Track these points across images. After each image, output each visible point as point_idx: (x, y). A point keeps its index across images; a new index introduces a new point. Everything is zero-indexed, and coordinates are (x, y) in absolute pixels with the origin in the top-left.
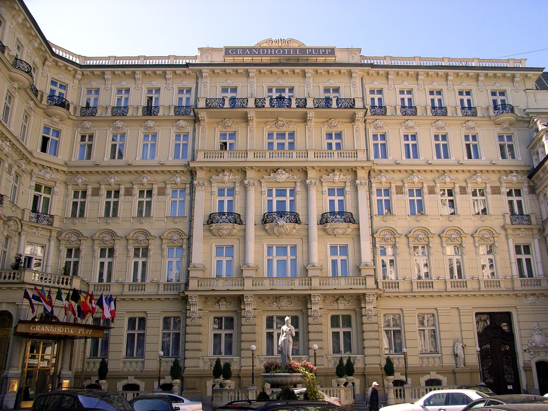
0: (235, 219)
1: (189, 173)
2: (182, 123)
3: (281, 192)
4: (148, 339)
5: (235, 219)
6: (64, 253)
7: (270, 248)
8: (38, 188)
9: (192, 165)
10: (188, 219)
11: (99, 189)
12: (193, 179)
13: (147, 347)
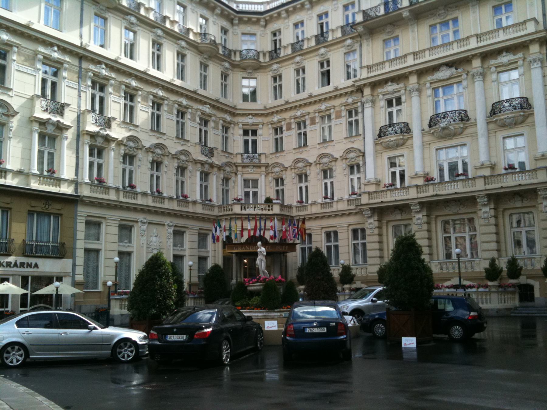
0: (401, 129)
1: (360, 91)
2: (349, 42)
4: (341, 250)
5: (401, 129)
6: (274, 182)
8: (246, 133)
10: (362, 136)
12: (363, 97)
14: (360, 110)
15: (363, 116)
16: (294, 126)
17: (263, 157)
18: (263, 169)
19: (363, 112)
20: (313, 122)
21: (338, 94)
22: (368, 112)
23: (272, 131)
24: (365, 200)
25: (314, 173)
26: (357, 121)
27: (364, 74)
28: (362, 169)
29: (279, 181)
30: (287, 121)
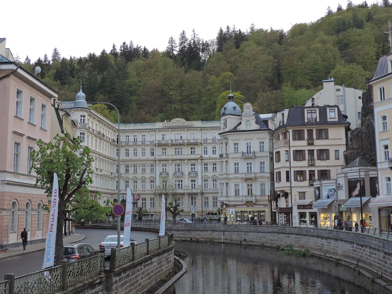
2: (152, 146)
3: (179, 165)
7: (176, 181)
9: (155, 159)
11: (132, 165)
13: (147, 206)
14: (154, 166)
15: (156, 168)
16: (133, 166)
17: (122, 174)
18: (122, 178)
19: (156, 166)
20: (139, 166)
21: (147, 160)
22: (157, 167)
23: (125, 166)
24: (157, 192)
25: (139, 181)
26: (153, 168)
27: (157, 157)
28: (154, 182)
29: (127, 182)
30: (131, 164)
